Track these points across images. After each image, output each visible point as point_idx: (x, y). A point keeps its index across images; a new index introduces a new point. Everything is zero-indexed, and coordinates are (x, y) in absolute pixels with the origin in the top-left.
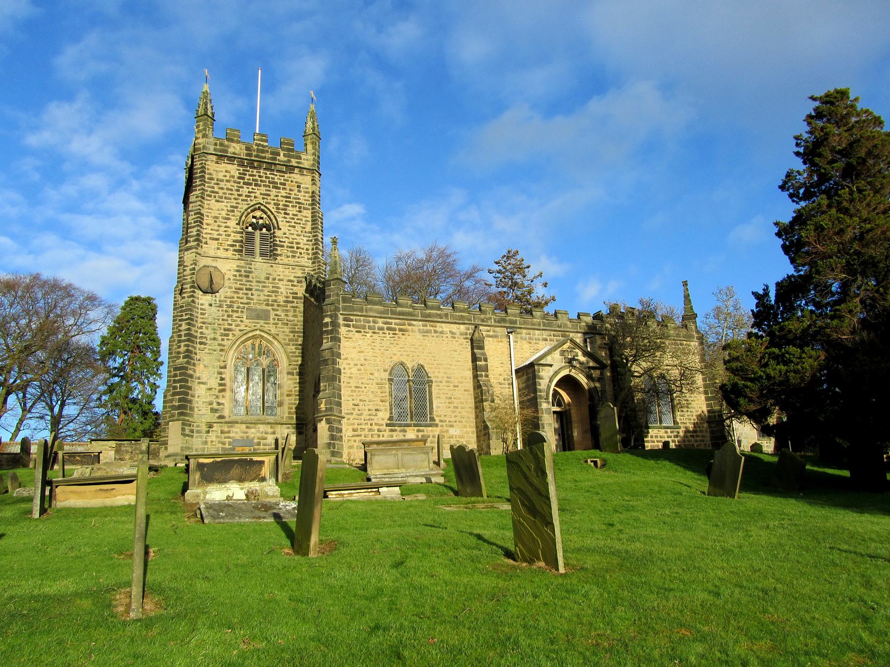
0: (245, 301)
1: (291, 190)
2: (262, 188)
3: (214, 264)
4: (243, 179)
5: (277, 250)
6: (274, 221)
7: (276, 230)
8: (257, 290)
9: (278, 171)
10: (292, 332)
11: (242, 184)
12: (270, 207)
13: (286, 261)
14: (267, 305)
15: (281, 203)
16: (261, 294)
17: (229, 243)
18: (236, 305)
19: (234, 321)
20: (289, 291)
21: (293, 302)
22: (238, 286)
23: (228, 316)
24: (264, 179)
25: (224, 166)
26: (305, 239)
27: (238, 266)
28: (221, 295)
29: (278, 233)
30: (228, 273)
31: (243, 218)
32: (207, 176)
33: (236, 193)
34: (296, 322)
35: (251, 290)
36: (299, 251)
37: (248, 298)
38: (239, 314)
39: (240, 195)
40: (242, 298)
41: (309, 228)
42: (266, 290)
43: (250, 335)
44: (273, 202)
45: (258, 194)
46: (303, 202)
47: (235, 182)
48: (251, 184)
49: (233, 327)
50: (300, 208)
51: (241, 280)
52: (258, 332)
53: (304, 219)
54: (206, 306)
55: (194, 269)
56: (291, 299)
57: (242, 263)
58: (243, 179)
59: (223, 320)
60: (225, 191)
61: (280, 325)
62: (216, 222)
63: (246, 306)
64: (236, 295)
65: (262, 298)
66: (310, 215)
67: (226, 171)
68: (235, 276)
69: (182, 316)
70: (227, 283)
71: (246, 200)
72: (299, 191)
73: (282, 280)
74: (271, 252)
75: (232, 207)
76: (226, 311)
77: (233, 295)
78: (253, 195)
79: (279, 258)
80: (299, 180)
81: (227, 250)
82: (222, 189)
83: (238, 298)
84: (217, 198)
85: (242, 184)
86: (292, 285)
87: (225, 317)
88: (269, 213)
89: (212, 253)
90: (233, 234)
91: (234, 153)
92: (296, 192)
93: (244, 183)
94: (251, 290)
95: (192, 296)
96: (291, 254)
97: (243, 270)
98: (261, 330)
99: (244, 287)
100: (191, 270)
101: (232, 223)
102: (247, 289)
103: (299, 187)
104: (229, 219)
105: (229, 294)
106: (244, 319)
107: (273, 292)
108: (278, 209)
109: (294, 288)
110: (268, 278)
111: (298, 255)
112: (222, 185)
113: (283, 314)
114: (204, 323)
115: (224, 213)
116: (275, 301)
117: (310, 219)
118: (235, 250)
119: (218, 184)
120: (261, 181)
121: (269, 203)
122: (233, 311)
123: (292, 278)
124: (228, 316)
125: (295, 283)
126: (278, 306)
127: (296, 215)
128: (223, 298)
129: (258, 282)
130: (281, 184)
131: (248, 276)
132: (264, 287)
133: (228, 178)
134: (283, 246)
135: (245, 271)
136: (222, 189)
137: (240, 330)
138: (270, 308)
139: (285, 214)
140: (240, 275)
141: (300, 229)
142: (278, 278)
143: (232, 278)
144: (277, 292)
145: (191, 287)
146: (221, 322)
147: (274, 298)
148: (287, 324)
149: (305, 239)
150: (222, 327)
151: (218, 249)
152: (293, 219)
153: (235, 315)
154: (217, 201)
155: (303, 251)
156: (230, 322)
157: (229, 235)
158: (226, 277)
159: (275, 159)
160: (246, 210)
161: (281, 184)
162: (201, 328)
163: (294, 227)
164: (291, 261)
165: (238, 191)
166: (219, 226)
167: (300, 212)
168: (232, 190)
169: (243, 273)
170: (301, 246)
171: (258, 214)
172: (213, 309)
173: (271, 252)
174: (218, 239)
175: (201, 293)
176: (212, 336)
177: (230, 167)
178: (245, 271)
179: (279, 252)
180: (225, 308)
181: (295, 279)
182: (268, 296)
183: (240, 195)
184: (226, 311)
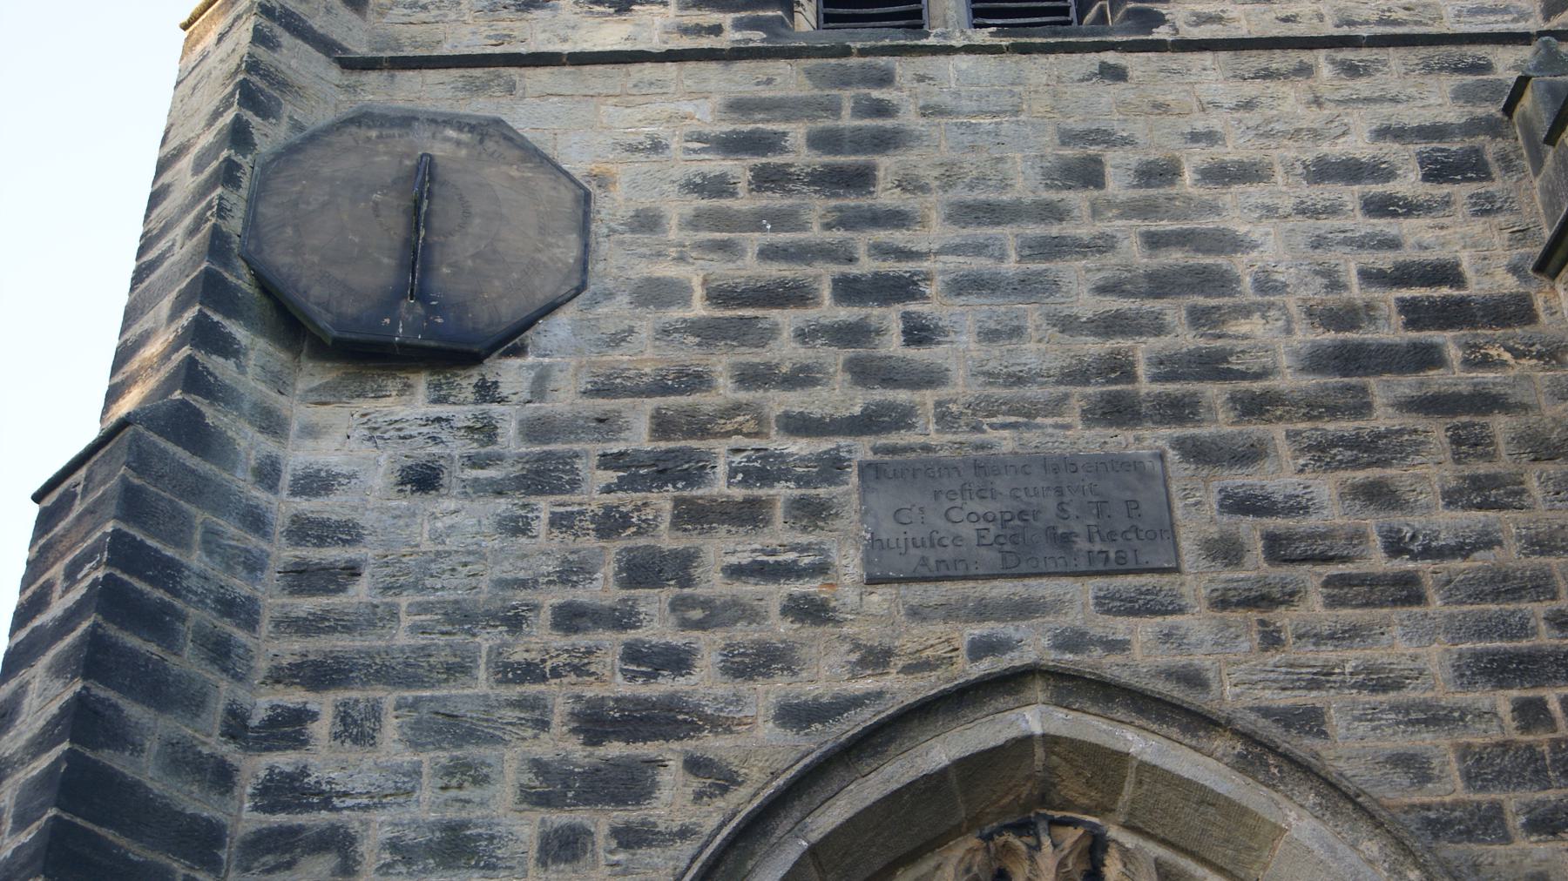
8: (965, 285)
10: (1499, 670)
14: (1118, 411)
16: (1032, 315)
18: (722, 453)
19: (715, 615)
21: (1427, 357)
22: (749, 268)
23: (642, 571)
27: (739, 107)
28: (555, 369)
34: (1510, 556)
35: (899, 289)
37: (863, 373)
38: (779, 536)
40: (801, 378)
43: (939, 750)
49: (703, 683)
51: (782, 220)
52: (1034, 717)
56: (1390, 331)
59: (570, 618)
61: (1314, 609)
63: (861, 448)
64: (721, 363)
65: (1039, 351)
70: (618, 261)
73: (1247, 173)
76: (611, 524)
77: (688, 354)
83: (750, 377)
86: (1379, 207)
87: (602, 589)
94: (899, 289)
98: (1071, 686)
99: (823, 274)
105: (645, 355)
106: (846, 583)
107: (1161, 284)
110: (1088, 174)
113: (1325, 488)
114: (321, 674)
116: (1212, 366)
123: (1359, 145)
124: (642, 571)
125: (1409, 184)
126: (1254, 407)
128: (565, 400)
132: (1054, 248)
137: (796, 715)
138: (1152, 439)
140: (766, 179)
144: (1218, 282)
146: (540, 640)
147: (1185, 339)
148: (1407, 591)
150: (559, 696)
153: (721, 548)
156: (658, 629)
158: (613, 206)
162: (288, 728)
172: (458, 517)
175: (313, 375)
176: (428, 808)
180: (595, 489)
184: (611, 524)
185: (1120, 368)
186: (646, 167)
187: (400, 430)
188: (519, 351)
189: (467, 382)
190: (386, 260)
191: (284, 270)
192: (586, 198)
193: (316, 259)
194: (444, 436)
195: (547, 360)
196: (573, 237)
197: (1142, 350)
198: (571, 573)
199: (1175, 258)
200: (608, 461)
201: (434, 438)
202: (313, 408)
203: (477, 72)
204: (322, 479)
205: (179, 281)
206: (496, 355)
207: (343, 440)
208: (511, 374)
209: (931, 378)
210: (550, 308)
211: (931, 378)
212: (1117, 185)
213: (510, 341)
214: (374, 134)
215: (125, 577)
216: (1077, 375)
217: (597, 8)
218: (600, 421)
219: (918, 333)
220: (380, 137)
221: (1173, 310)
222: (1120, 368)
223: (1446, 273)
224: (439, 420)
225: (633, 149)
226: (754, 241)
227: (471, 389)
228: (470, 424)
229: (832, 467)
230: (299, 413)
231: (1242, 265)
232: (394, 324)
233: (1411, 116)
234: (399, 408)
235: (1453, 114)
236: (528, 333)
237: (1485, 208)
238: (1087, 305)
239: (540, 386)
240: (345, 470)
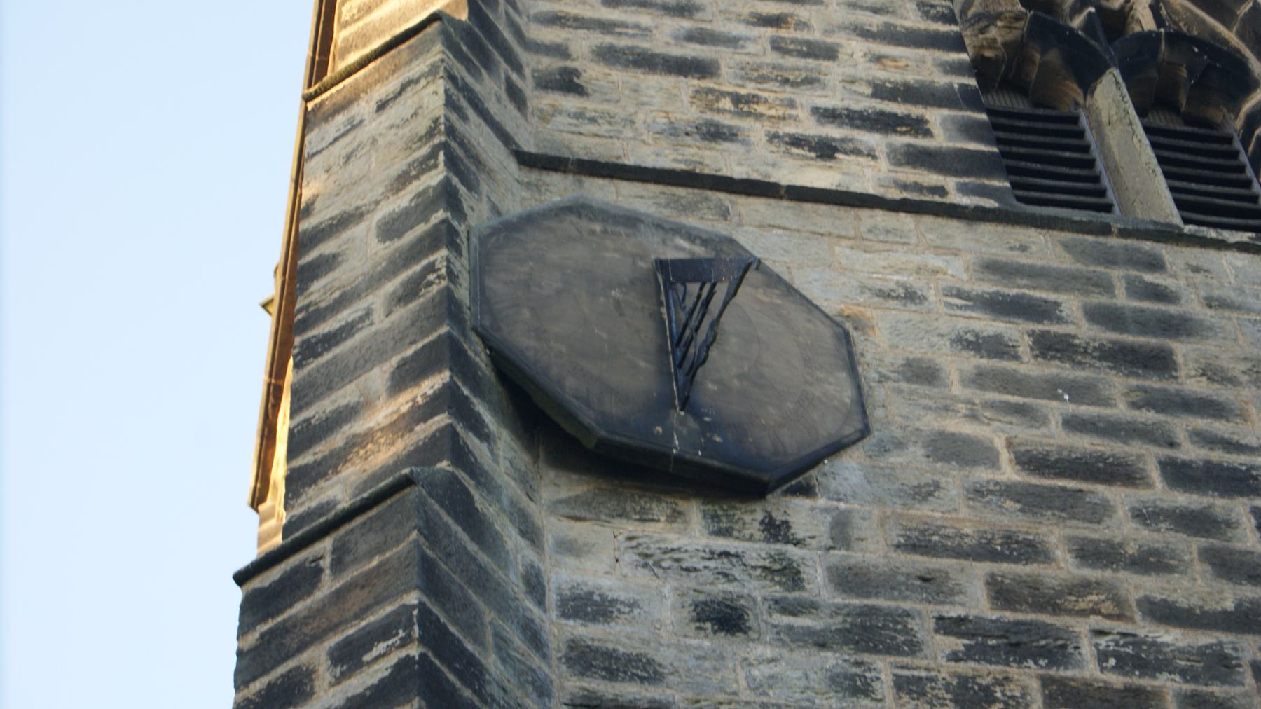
22: (1053, 436)
28: (849, 516)
51: (1080, 392)
64: (1055, 534)
83: (1089, 553)
90: (856, 48)
97: (1071, 304)
100: (389, 230)
128: (874, 550)
140: (1048, 347)
143: (957, 367)
186: (905, 316)
187: (678, 560)
188: (807, 491)
189: (751, 517)
190: (642, 364)
191: (530, 354)
192: (846, 339)
193: (564, 349)
194: (737, 572)
195: (842, 505)
196: (843, 375)
200: (947, 626)
201: (726, 575)
202: (566, 523)
203: (681, 191)
204: (596, 604)
205: (395, 350)
206: (779, 491)
207: (617, 565)
208: (802, 514)
210: (836, 448)
213: (796, 475)
214: (598, 227)
215: (437, 663)
217: (795, 150)
218: (924, 580)
220: (605, 232)
224: (726, 554)
225: (886, 295)
226: (1056, 410)
227: (757, 525)
228: (767, 563)
230: (553, 527)
232: (668, 435)
234: (671, 536)
236: (813, 473)
239: (841, 532)
240: (623, 596)
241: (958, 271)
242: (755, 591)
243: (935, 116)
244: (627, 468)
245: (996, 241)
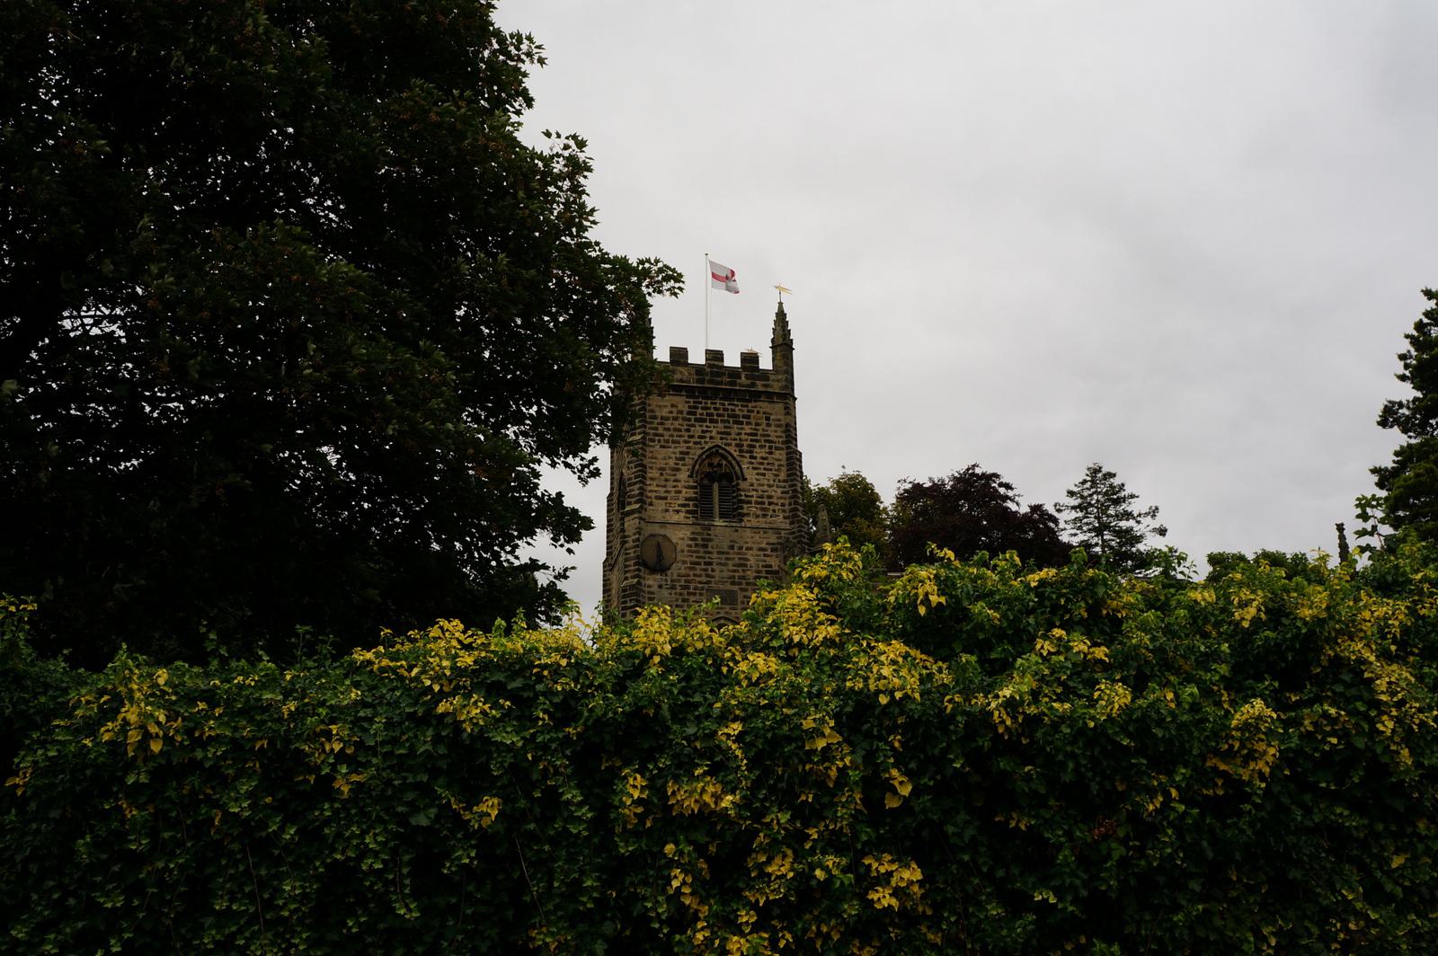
0: (704, 579)
1: (757, 424)
2: (720, 425)
3: (662, 532)
4: (695, 414)
5: (742, 508)
6: (737, 468)
7: (740, 481)
9: (738, 400)
11: (693, 422)
12: (731, 449)
13: (754, 522)
14: (733, 583)
15: (745, 443)
16: (725, 568)
17: (680, 502)
18: (692, 586)
20: (761, 564)
22: (694, 559)
24: (721, 412)
25: (669, 400)
26: (779, 490)
27: (693, 533)
29: (743, 485)
30: (680, 542)
31: (697, 467)
32: (648, 414)
33: (687, 434)
35: (710, 564)
36: (771, 507)
37: (707, 576)
38: (697, 597)
39: (692, 437)
40: (700, 576)
41: (783, 476)
42: (730, 562)
44: (734, 443)
45: (713, 434)
46: (775, 439)
47: (684, 419)
48: (705, 421)
50: (770, 448)
53: (776, 463)
54: (655, 589)
55: (638, 540)
57: (699, 529)
58: (695, 414)
60: (672, 432)
62: (662, 474)
63: (706, 586)
64: (691, 573)
65: (725, 574)
66: (784, 457)
67: (672, 406)
68: (690, 546)
69: (626, 602)
70: (679, 558)
71: (699, 443)
72: (768, 425)
73: (751, 549)
74: (733, 512)
75: (681, 453)
76: (681, 594)
78: (708, 435)
79: (746, 519)
80: (768, 410)
81: (678, 512)
82: (668, 429)
83: (695, 575)
84: (662, 443)
85: (693, 422)
86: (765, 555)
87: (680, 603)
88: (730, 458)
89: (659, 517)
90: (684, 490)
91: (681, 381)
92: (764, 426)
93: (696, 420)
94: (710, 564)
95: (637, 576)
96: (759, 512)
97: (699, 538)
99: (702, 560)
100: (634, 541)
101: (683, 475)
102: (706, 563)
103: (768, 419)
104: (678, 470)
105: (683, 571)
107: (740, 565)
108: (741, 451)
109: (768, 559)
110: (732, 547)
111: (770, 513)
112: (668, 424)
115: (672, 463)
116: (743, 577)
117: (784, 463)
118: (688, 512)
119: (662, 424)
120: (718, 415)
121: (730, 445)
122: (689, 594)
123: (763, 546)
124: (684, 600)
125: (769, 552)
126: (748, 584)
127: (765, 459)
128: (675, 577)
129: (719, 553)
130: (744, 417)
131: (706, 546)
132: (727, 559)
133: (675, 415)
134: (750, 502)
135: (703, 539)
136: (668, 429)
138: (736, 588)
139: (751, 457)
140: (696, 545)
141: (772, 478)
142: (745, 546)
144: (745, 565)
145: (635, 564)
147: (741, 574)
149: (779, 490)
151: (667, 511)
152: (762, 464)
154: (662, 447)
155: (777, 508)
157: (680, 492)
158: (679, 548)
159: (734, 384)
160: (700, 456)
161: (744, 417)
163: (764, 475)
164: (762, 522)
165: (688, 430)
166: (666, 480)
167: (771, 453)
168: (680, 430)
169: (700, 542)
170: (775, 500)
171: (716, 461)
173: (733, 512)
174: (665, 498)
175: (648, 571)
177: (676, 399)
178: (703, 539)
179: (745, 511)
181: (769, 547)
182: (734, 571)
183: (692, 437)
184: (681, 594)
185: (734, 577)
197: (737, 574)
198: (677, 600)
199: (742, 562)
208: (669, 572)
209: (714, 577)
211: (714, 577)
212: (736, 550)
216: (730, 578)
219: (713, 570)
221: (740, 569)
222: (734, 577)
223: (771, 566)
229: (703, 588)
231: (749, 563)
233: (771, 541)
235: (776, 541)
237: (777, 557)
238: (731, 568)
241: (688, 533)
242: (664, 583)
243: (691, 503)
244: (653, 571)
245: (692, 529)
